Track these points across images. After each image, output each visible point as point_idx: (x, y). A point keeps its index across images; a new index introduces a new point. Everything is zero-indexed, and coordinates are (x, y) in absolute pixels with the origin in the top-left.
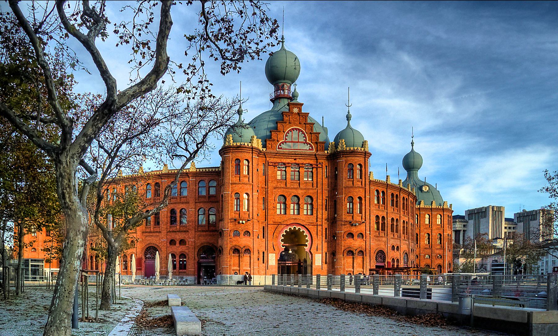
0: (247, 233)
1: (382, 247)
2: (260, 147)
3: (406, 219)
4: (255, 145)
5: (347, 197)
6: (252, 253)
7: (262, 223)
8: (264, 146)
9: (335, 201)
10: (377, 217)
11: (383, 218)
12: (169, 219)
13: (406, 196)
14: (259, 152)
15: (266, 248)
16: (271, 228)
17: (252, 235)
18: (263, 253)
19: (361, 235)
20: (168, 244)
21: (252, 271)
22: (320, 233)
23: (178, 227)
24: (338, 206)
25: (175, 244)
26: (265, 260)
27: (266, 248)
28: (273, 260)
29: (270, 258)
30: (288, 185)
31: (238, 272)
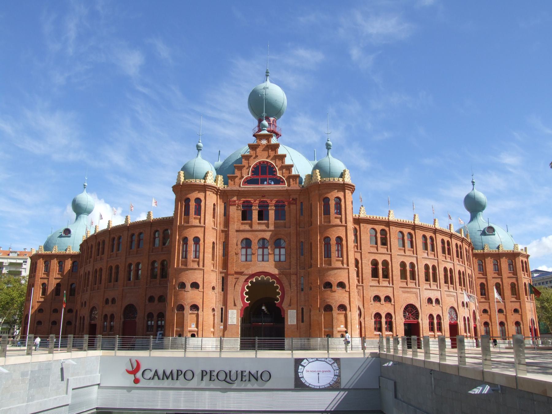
0: (195, 285)
1: (412, 300)
2: (220, 185)
3: (449, 266)
4: (210, 181)
5: (323, 238)
6: (200, 310)
7: (221, 273)
8: (226, 183)
9: (311, 243)
10: (403, 265)
11: (412, 265)
12: (149, 272)
13: (446, 239)
14: (217, 191)
15: (225, 303)
16: (231, 280)
17: (201, 287)
18: (222, 309)
19: (341, 285)
20: (147, 301)
21: (200, 333)
22: (293, 284)
23: (158, 281)
24: (313, 250)
25: (154, 302)
26: (224, 318)
27: (225, 303)
28: (234, 317)
29: (230, 315)
30: (256, 227)
31: (196, 333)
